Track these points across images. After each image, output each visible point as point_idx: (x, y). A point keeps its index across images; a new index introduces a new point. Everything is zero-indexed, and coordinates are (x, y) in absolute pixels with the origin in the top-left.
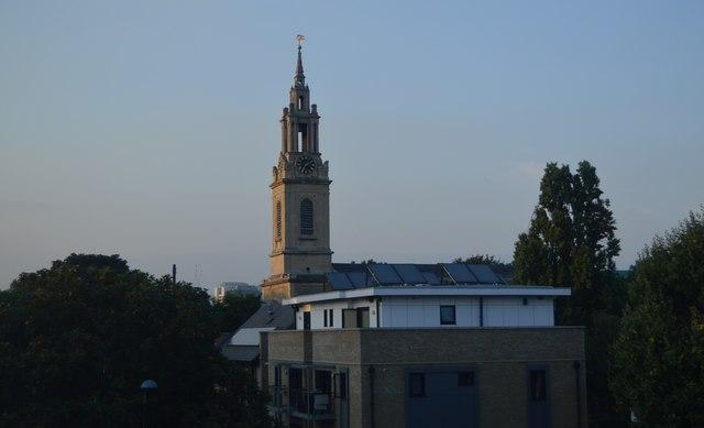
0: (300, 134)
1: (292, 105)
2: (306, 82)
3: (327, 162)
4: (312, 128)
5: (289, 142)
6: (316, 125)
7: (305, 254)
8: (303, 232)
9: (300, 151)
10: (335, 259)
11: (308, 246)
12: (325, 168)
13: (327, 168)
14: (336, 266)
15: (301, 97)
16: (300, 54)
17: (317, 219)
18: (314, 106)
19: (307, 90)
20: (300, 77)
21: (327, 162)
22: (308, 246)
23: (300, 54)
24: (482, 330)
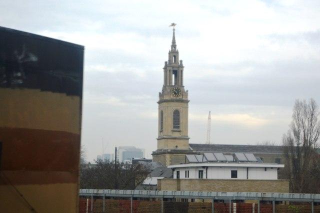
0: (173, 76)
1: (169, 61)
2: (177, 48)
3: (187, 91)
4: (180, 72)
5: (167, 79)
6: (182, 71)
7: (175, 138)
8: (174, 127)
9: (173, 84)
10: (191, 142)
11: (176, 135)
12: (186, 93)
13: (187, 94)
14: (191, 145)
15: (175, 56)
16: (174, 33)
17: (181, 121)
18: (181, 61)
19: (177, 53)
20: (174, 45)
21: (187, 91)
22: (176, 135)
23: (174, 33)
24: (247, 180)
